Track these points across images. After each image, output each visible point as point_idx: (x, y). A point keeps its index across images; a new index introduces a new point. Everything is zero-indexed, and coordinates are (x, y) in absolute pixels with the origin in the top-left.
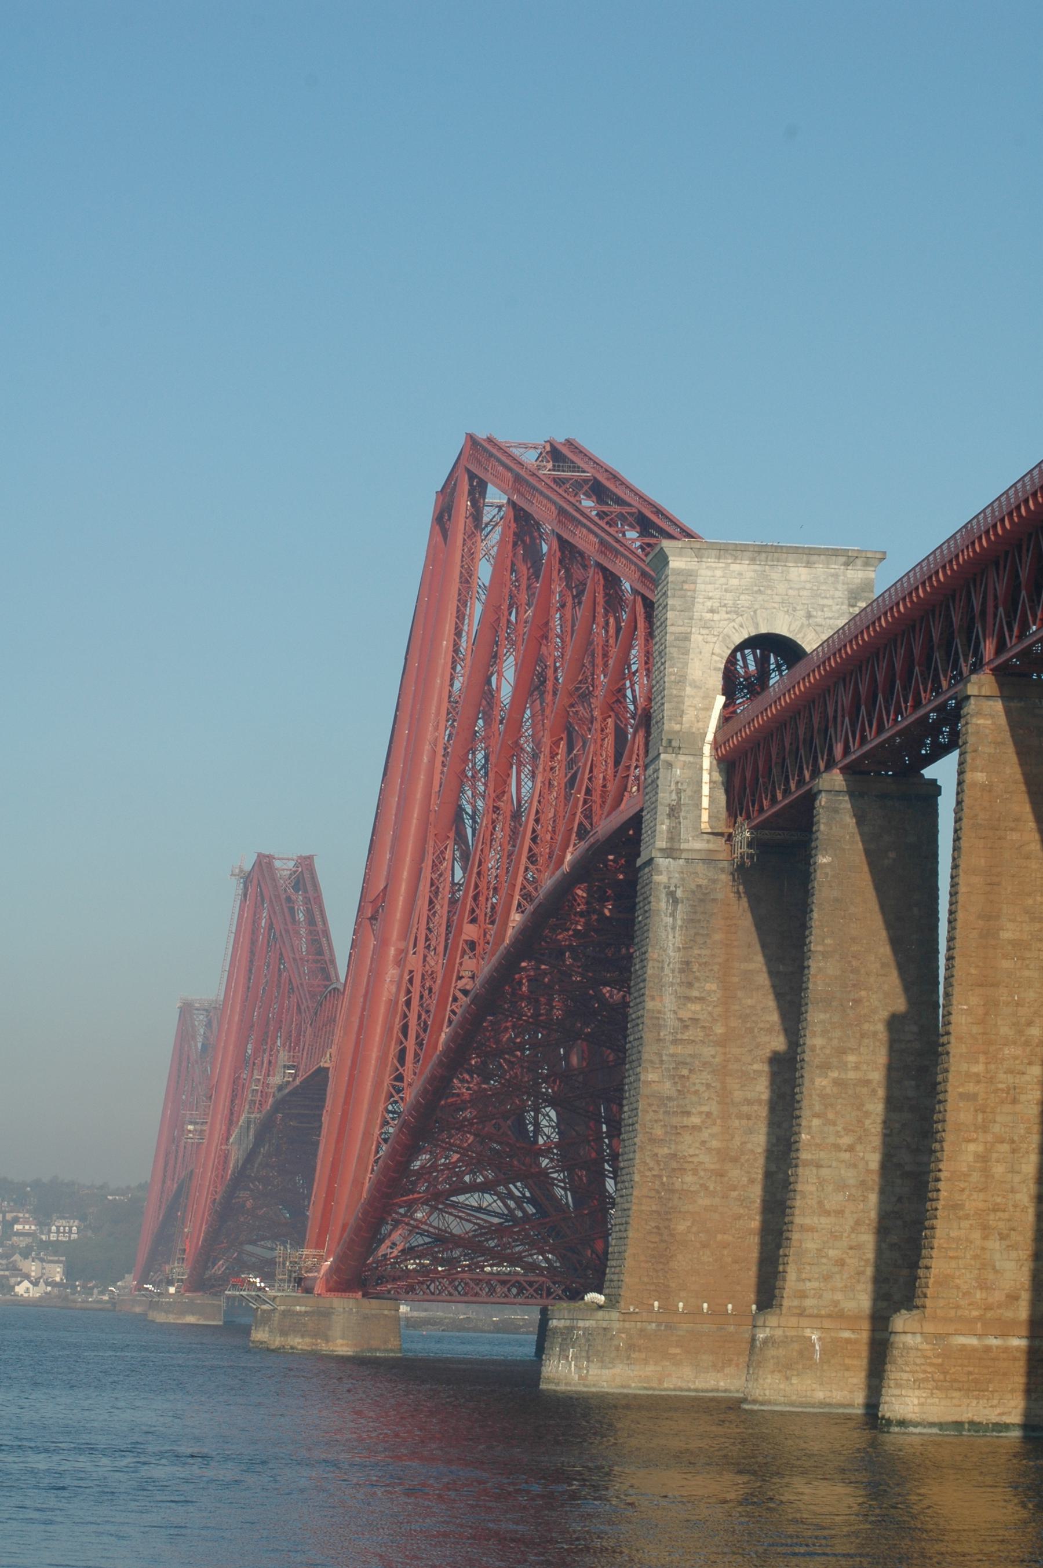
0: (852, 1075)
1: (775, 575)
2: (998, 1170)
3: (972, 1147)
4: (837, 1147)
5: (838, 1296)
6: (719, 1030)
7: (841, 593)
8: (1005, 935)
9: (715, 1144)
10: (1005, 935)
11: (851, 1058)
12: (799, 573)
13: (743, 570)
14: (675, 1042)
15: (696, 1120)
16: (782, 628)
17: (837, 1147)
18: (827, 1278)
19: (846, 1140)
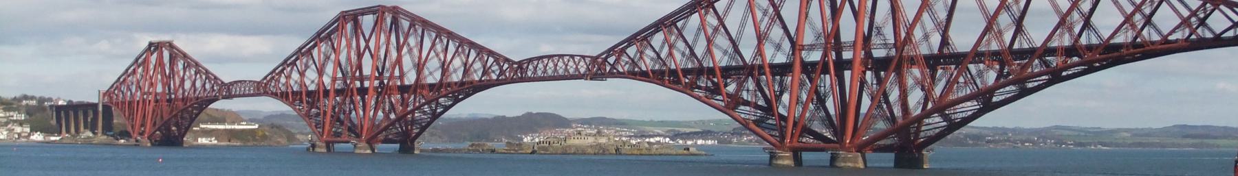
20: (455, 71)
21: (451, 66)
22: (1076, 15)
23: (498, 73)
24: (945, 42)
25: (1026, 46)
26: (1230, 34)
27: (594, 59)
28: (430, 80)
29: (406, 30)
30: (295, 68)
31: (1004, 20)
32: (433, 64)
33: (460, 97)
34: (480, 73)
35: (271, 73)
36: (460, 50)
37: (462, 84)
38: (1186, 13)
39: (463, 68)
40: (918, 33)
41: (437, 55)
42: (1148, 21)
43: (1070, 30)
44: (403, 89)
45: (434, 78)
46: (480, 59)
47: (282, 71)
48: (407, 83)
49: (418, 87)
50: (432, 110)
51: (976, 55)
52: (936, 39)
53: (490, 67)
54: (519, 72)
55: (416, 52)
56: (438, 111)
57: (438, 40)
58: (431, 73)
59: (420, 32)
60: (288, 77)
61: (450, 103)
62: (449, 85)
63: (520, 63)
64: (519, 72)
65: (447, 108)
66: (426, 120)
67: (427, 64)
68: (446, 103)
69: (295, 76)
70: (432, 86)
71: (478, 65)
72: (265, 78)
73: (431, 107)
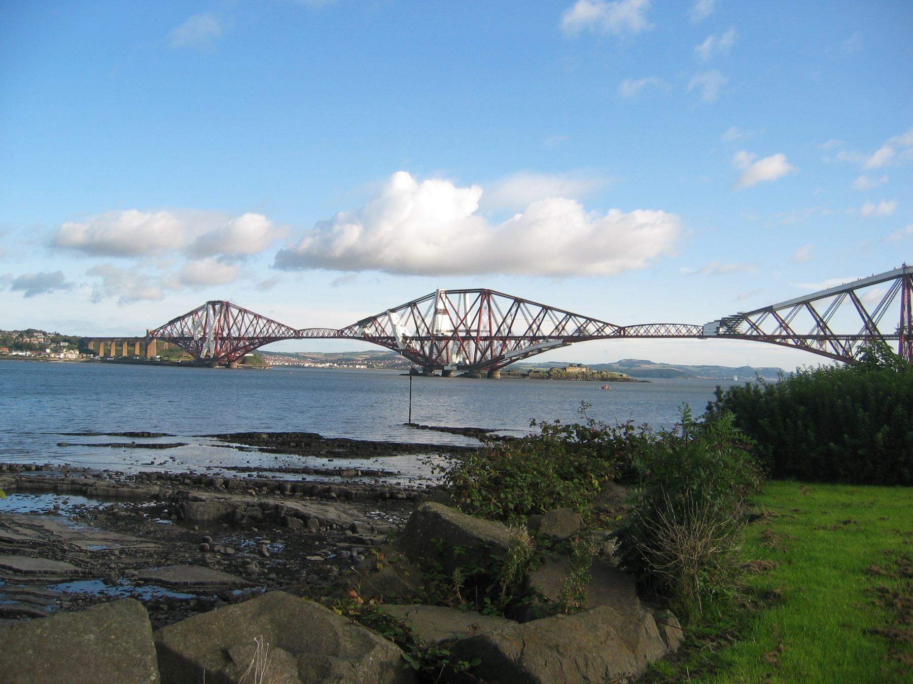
22: (560, 326)
24: (510, 332)
25: (541, 335)
26: (612, 334)
27: (338, 331)
31: (534, 327)
38: (598, 328)
40: (502, 328)
42: (563, 328)
43: (559, 330)
51: (524, 337)
52: (507, 331)
54: (298, 335)
63: (299, 331)
64: (298, 335)
71: (276, 331)
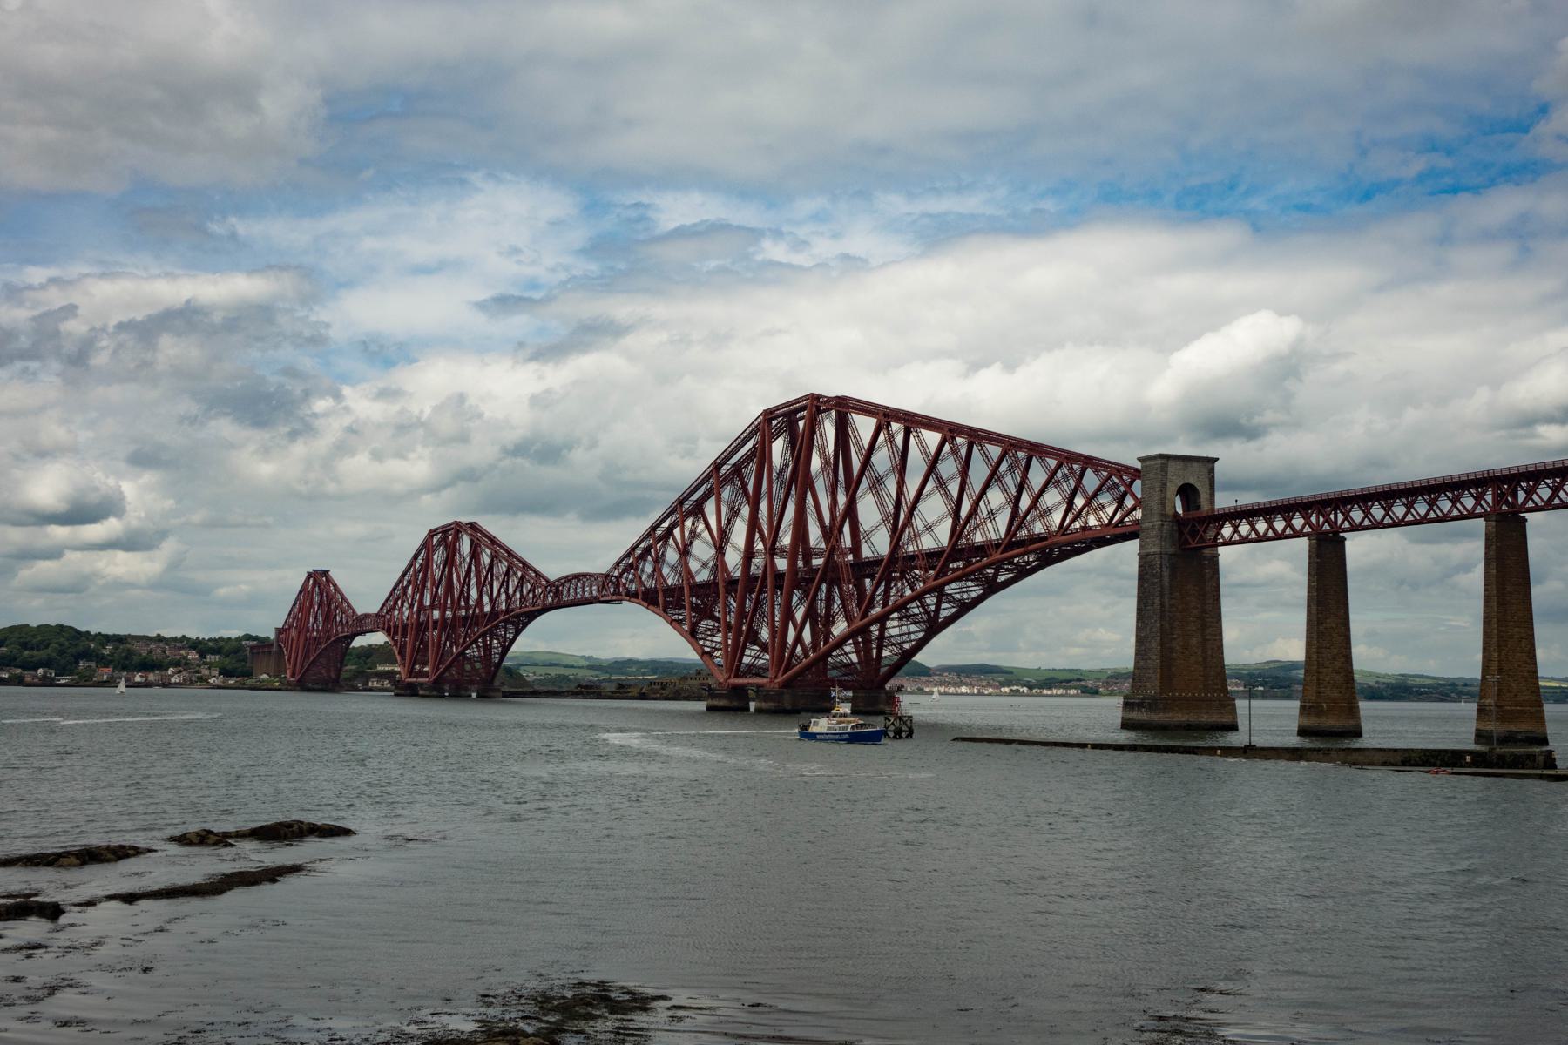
0: (1328, 625)
1: (1189, 464)
2: (1510, 658)
3: (1504, 651)
4: (1326, 648)
5: (1329, 693)
6: (1180, 607)
7: (1206, 471)
8: (1508, 590)
9: (1181, 644)
10: (1508, 590)
11: (1328, 621)
12: (1195, 465)
13: (1180, 464)
14: (1170, 612)
15: (1175, 636)
16: (1191, 481)
17: (1326, 648)
18: (1325, 687)
19: (1328, 645)
20: (992, 514)
21: (982, 503)
23: (1110, 510)
28: (927, 543)
29: (866, 439)
30: (671, 541)
32: (934, 509)
33: (1001, 578)
34: (1056, 518)
35: (628, 555)
36: (1004, 467)
37: (1011, 543)
39: (1009, 510)
41: (942, 485)
44: (863, 568)
45: (936, 538)
46: (1058, 483)
47: (647, 551)
48: (866, 552)
49: (898, 563)
50: (927, 612)
53: (1095, 495)
55: (891, 485)
56: (944, 614)
57: (947, 447)
58: (929, 528)
59: (899, 439)
60: (659, 561)
61: (974, 595)
62: (981, 550)
65: (965, 608)
66: (913, 637)
67: (921, 506)
68: (965, 596)
69: (672, 556)
70: (932, 556)
72: (618, 564)
73: (923, 606)
